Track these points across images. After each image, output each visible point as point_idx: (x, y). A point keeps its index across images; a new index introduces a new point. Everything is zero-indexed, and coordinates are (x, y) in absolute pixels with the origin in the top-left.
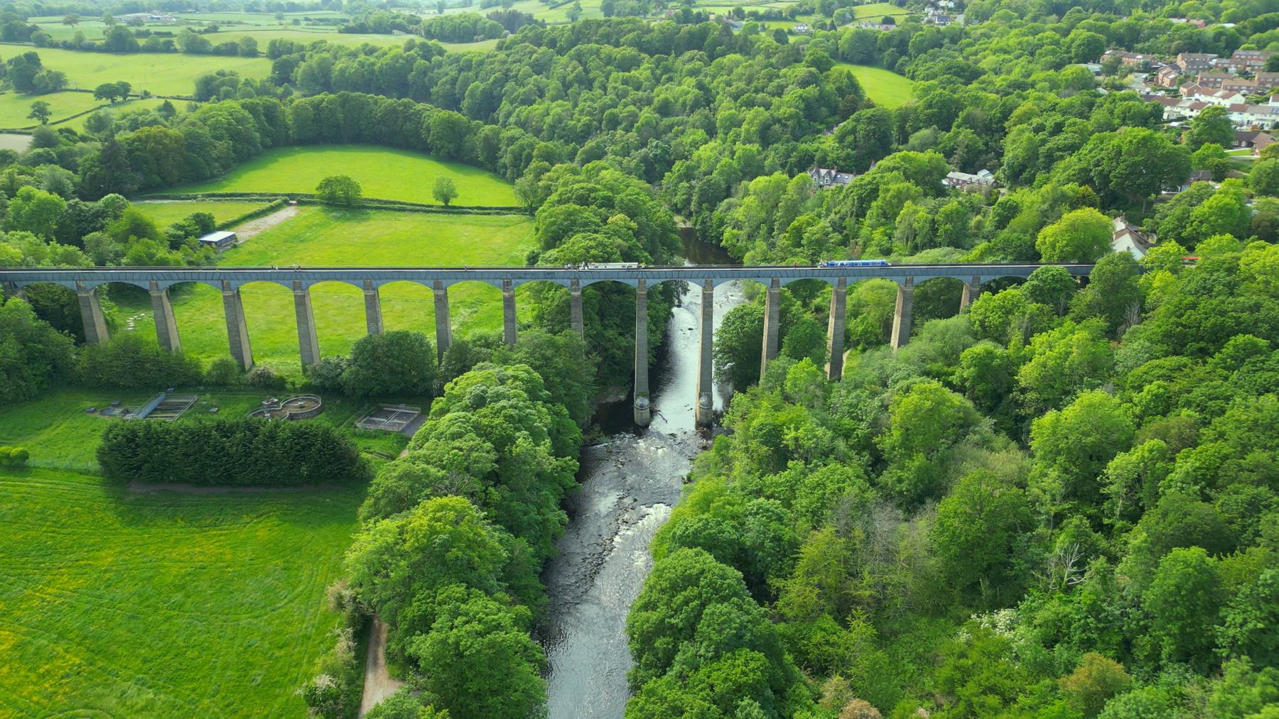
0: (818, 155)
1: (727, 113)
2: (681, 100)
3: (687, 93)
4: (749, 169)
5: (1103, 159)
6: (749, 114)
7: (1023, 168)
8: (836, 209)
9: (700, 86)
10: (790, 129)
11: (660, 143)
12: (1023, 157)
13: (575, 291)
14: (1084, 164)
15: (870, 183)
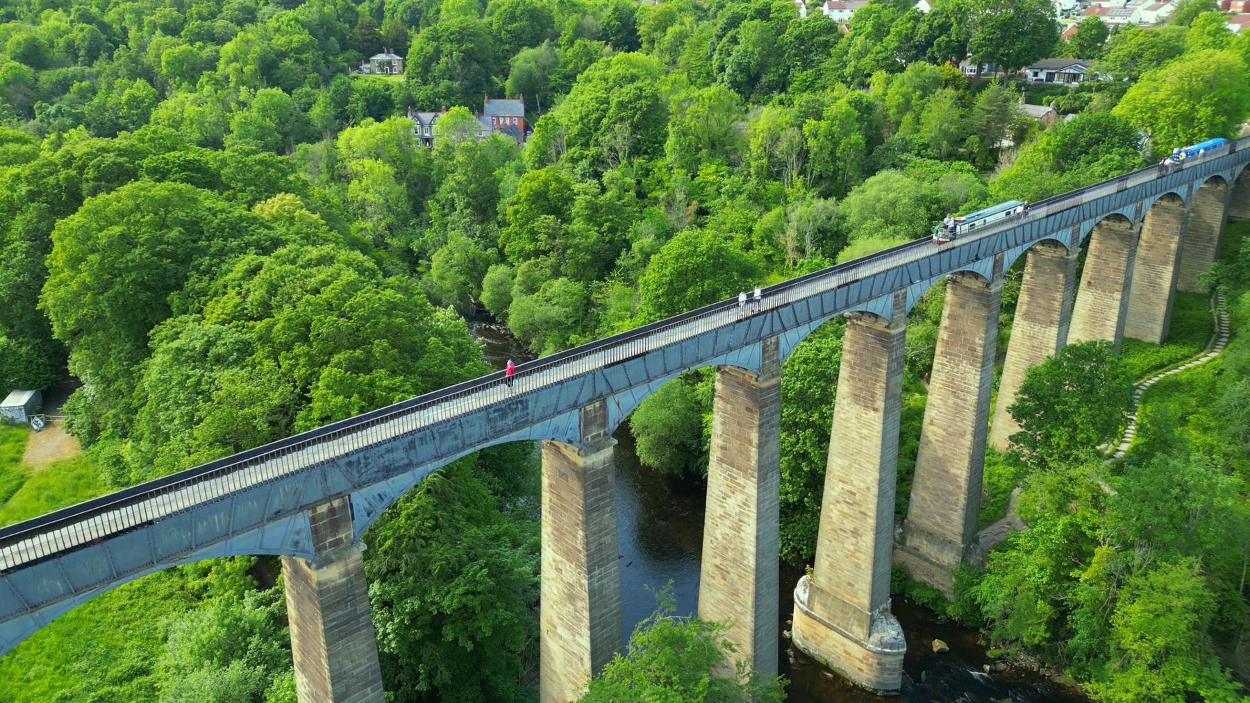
0: (397, 97)
1: (177, 50)
2: (61, 42)
3: (66, 32)
4: (288, 127)
5: (944, 28)
6: (228, 48)
7: (762, 67)
8: (575, 151)
9: (86, 18)
10: (310, 67)
11: (65, 108)
12: (759, 53)
13: (598, 448)
14: (891, 41)
15: (639, 98)
